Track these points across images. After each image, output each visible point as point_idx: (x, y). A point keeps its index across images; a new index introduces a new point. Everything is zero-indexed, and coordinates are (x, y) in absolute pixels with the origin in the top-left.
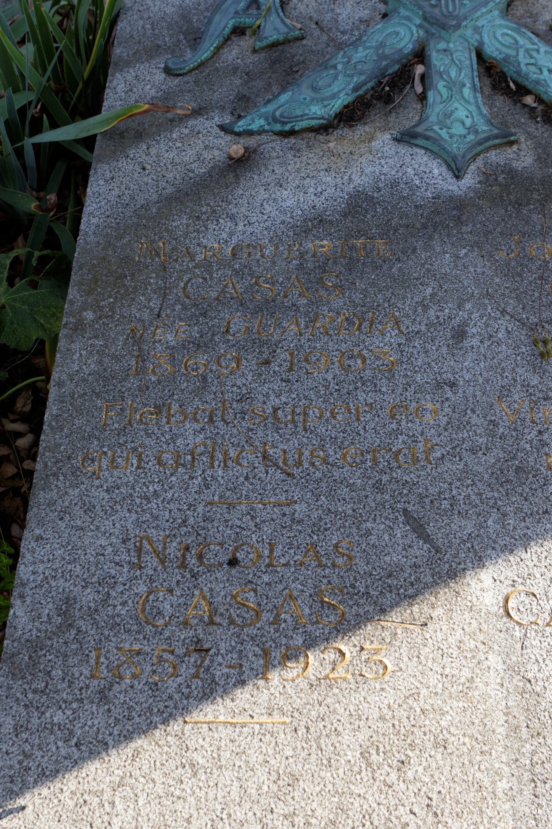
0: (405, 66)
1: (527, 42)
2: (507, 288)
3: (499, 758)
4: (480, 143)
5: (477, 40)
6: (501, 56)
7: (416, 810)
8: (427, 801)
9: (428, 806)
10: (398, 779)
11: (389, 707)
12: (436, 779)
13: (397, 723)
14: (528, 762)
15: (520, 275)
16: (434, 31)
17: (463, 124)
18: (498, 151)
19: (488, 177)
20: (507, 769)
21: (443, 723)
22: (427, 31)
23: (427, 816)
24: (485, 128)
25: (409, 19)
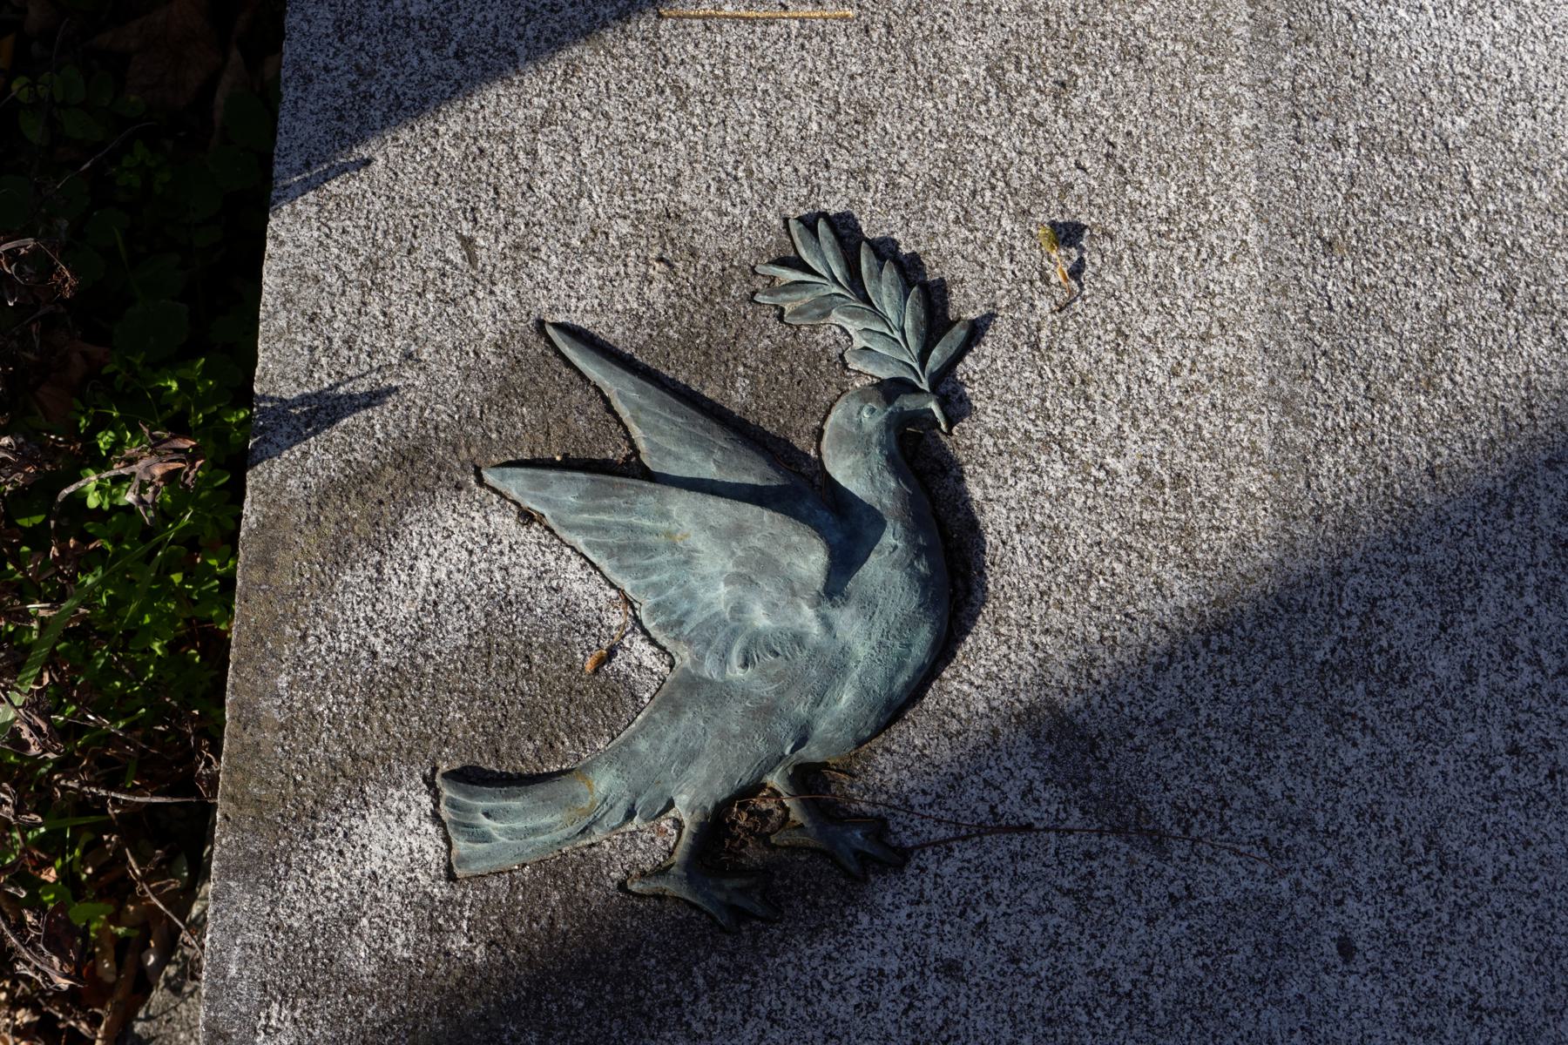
3: (1237, 77)
9: (1108, 156)
10: (1055, 112)
14: (1287, 84)
20: (1249, 95)
23: (1107, 172)
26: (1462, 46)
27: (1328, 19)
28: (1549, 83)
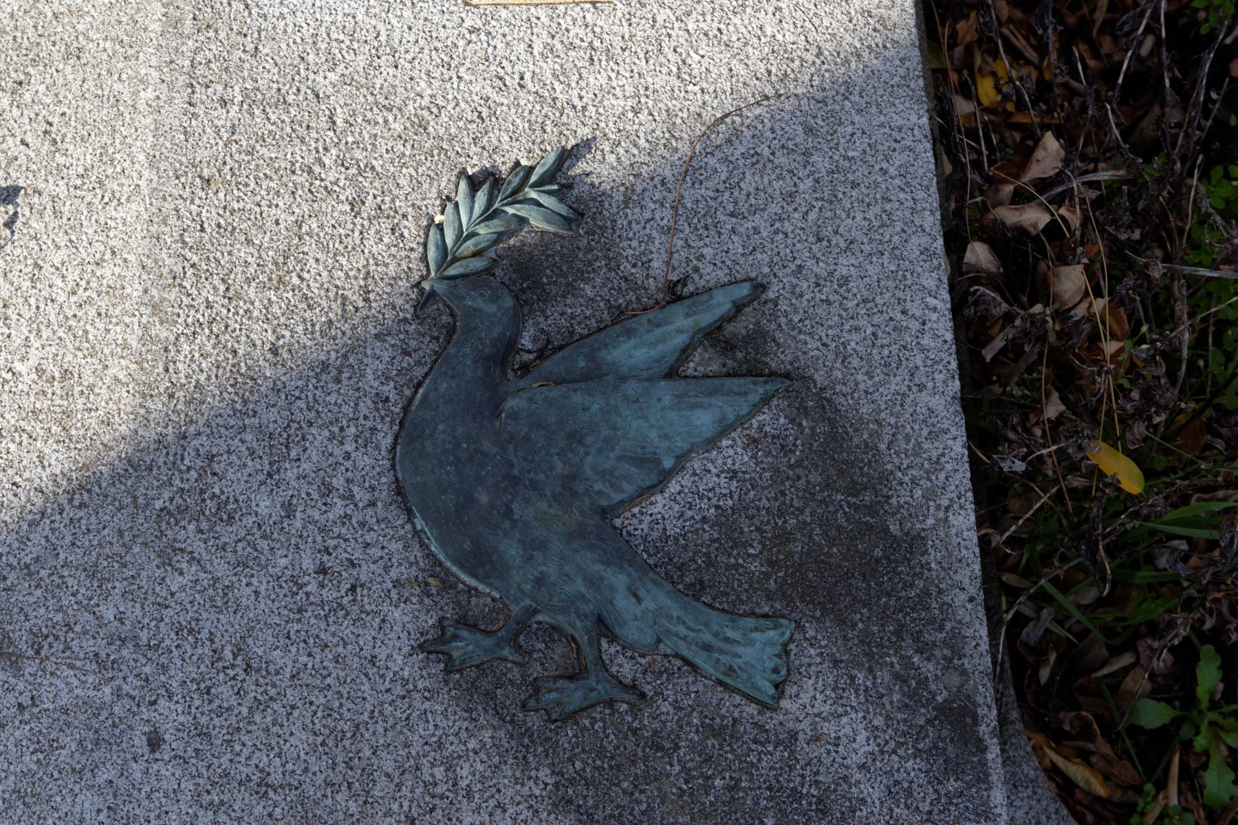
3: (148, 64)
7: (29, 140)
8: (45, 126)
9: (46, 132)
10: (11, 105)
11: (12, 16)
12: (61, 97)
13: (19, 34)
14: (187, 63)
20: (155, 74)
21: (80, 27)
23: (43, 144)
26: (340, 18)
27: (227, 9)
28: (412, 39)
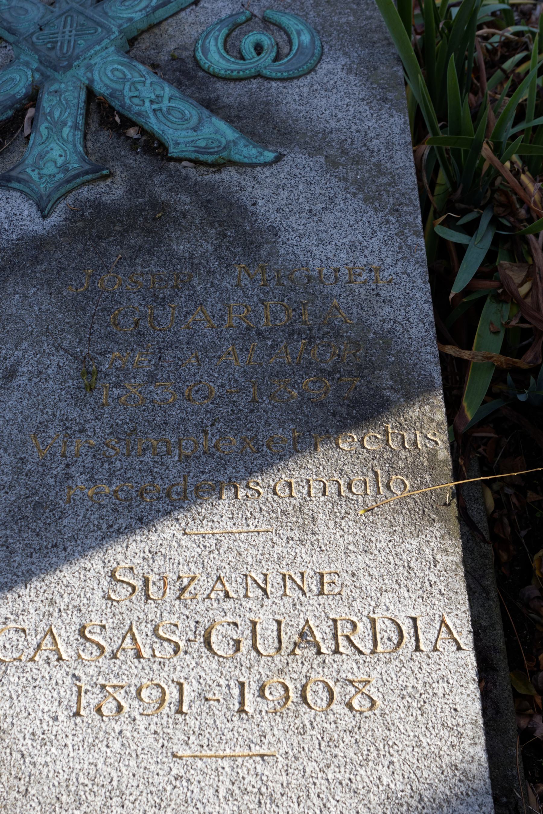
0: (17, 111)
1: (136, 74)
2: (68, 323)
4: (68, 181)
5: (88, 78)
6: (108, 92)
15: (84, 309)
16: (48, 73)
17: (55, 163)
18: (91, 186)
19: (74, 215)
22: (42, 74)
24: (76, 165)
25: (27, 64)
26: (86, 766)
27: (9, 758)
28: (135, 784)
